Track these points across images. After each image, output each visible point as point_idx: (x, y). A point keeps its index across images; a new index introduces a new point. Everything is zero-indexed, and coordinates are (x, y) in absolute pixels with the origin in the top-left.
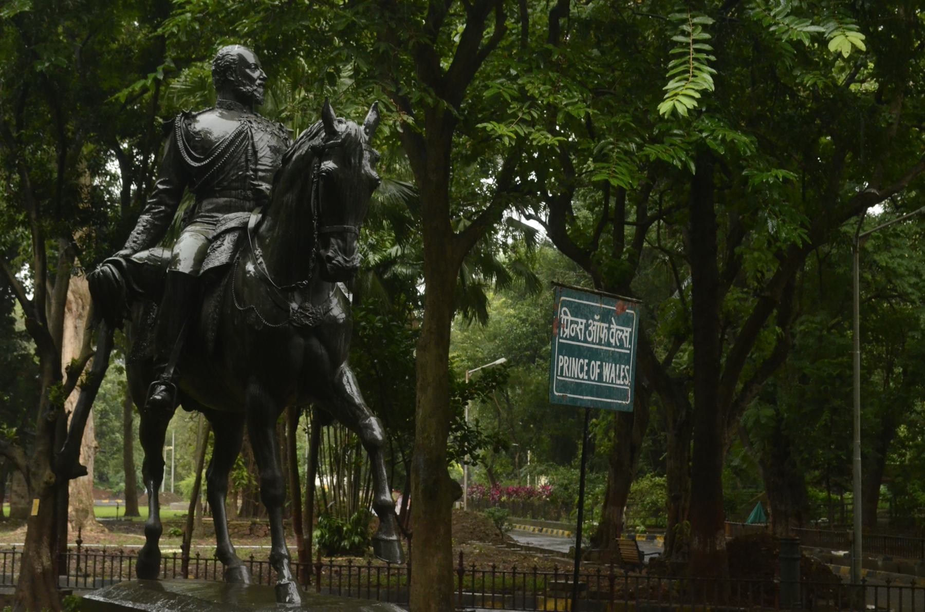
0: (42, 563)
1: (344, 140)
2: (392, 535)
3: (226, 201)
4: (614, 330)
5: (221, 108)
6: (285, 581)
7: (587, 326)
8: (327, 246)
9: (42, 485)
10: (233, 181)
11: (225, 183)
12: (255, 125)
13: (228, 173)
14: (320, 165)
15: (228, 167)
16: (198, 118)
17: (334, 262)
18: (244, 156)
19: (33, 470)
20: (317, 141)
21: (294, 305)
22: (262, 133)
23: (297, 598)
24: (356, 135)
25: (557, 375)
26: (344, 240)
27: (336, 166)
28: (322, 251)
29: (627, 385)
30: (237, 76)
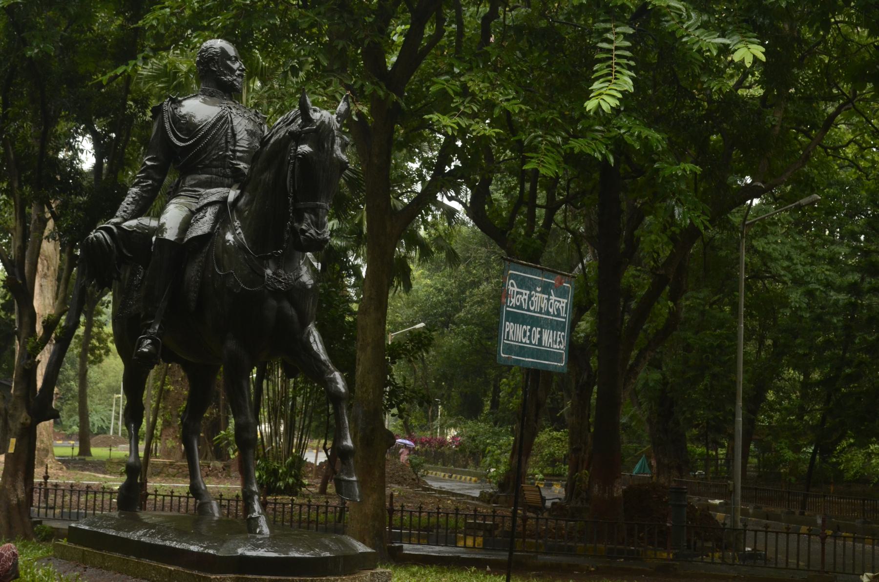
0: (17, 495)
1: (319, 127)
2: (352, 476)
3: (207, 178)
4: (552, 301)
5: (203, 95)
6: (255, 515)
7: (530, 297)
8: (301, 220)
9: (19, 426)
10: (214, 160)
11: (207, 162)
12: (234, 111)
13: (210, 153)
14: (297, 148)
15: (210, 147)
16: (184, 103)
17: (307, 234)
18: (224, 138)
19: (11, 412)
20: (294, 127)
21: (269, 272)
22: (240, 118)
23: (266, 530)
24: (329, 122)
25: (504, 339)
26: (316, 215)
27: (311, 150)
28: (296, 224)
29: (562, 350)
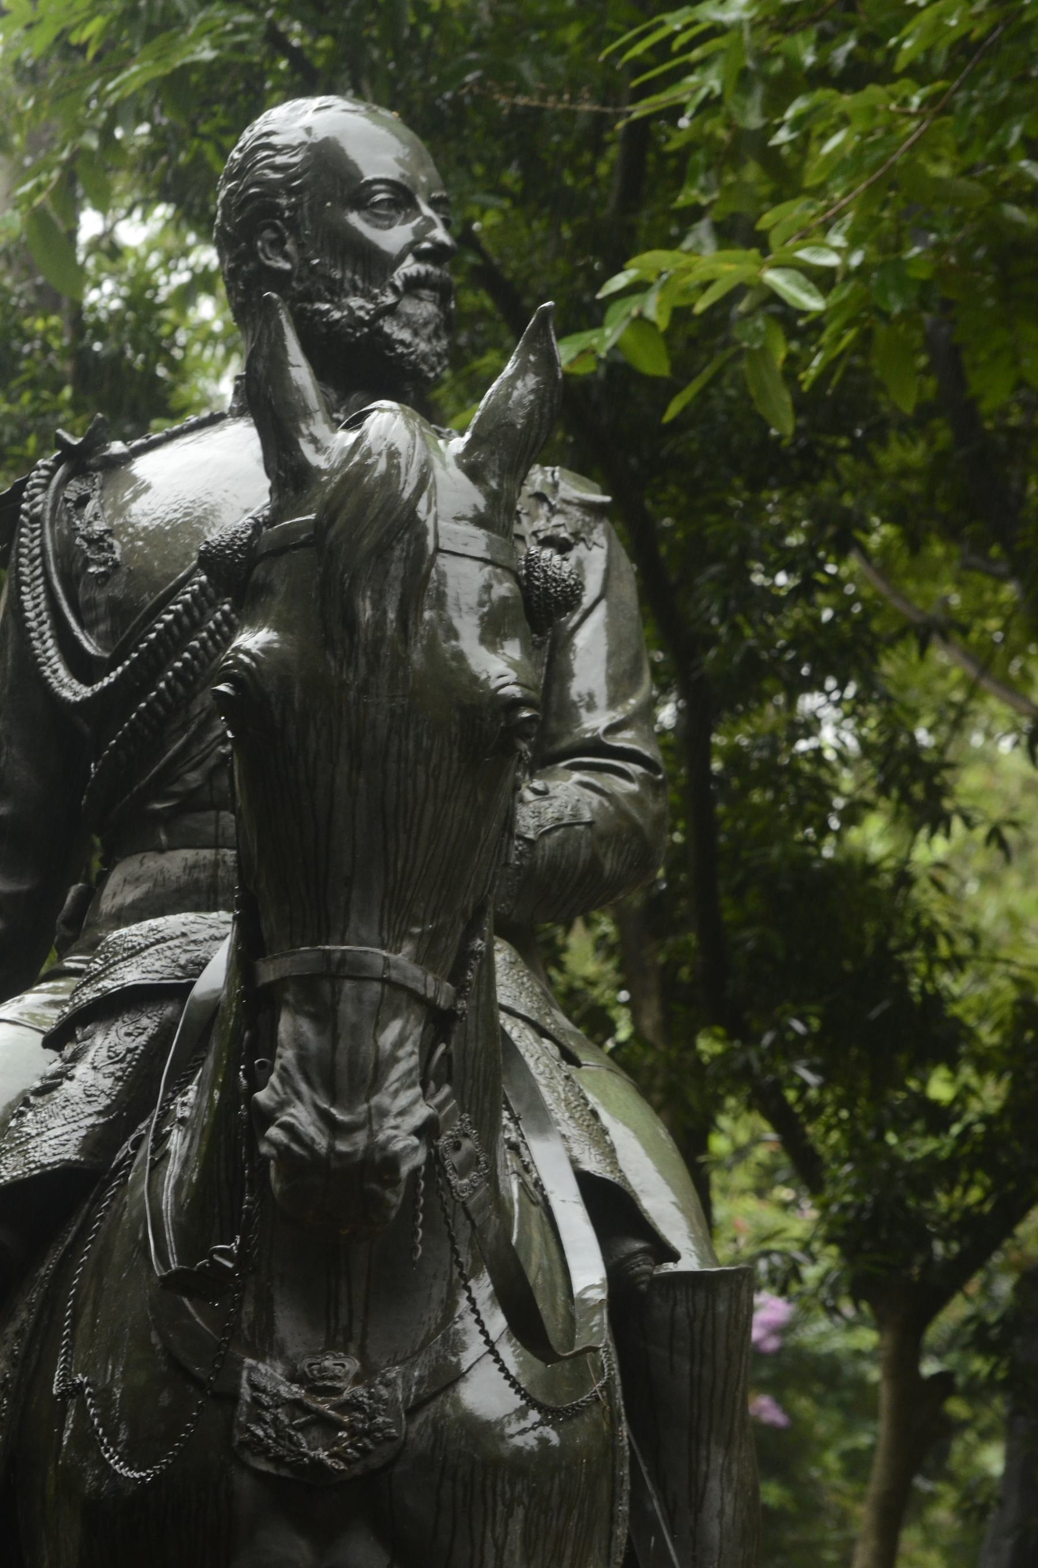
3: (194, 866)
11: (194, 778)
16: (143, 467)
30: (300, 246)
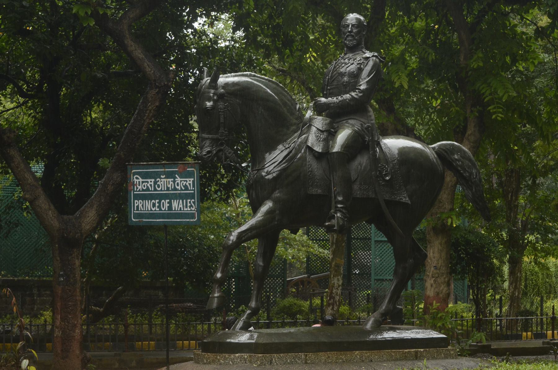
4: (179, 182)
7: (155, 183)
29: (194, 210)
